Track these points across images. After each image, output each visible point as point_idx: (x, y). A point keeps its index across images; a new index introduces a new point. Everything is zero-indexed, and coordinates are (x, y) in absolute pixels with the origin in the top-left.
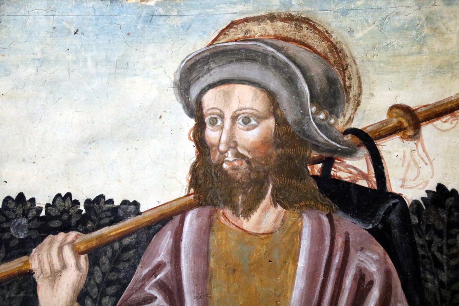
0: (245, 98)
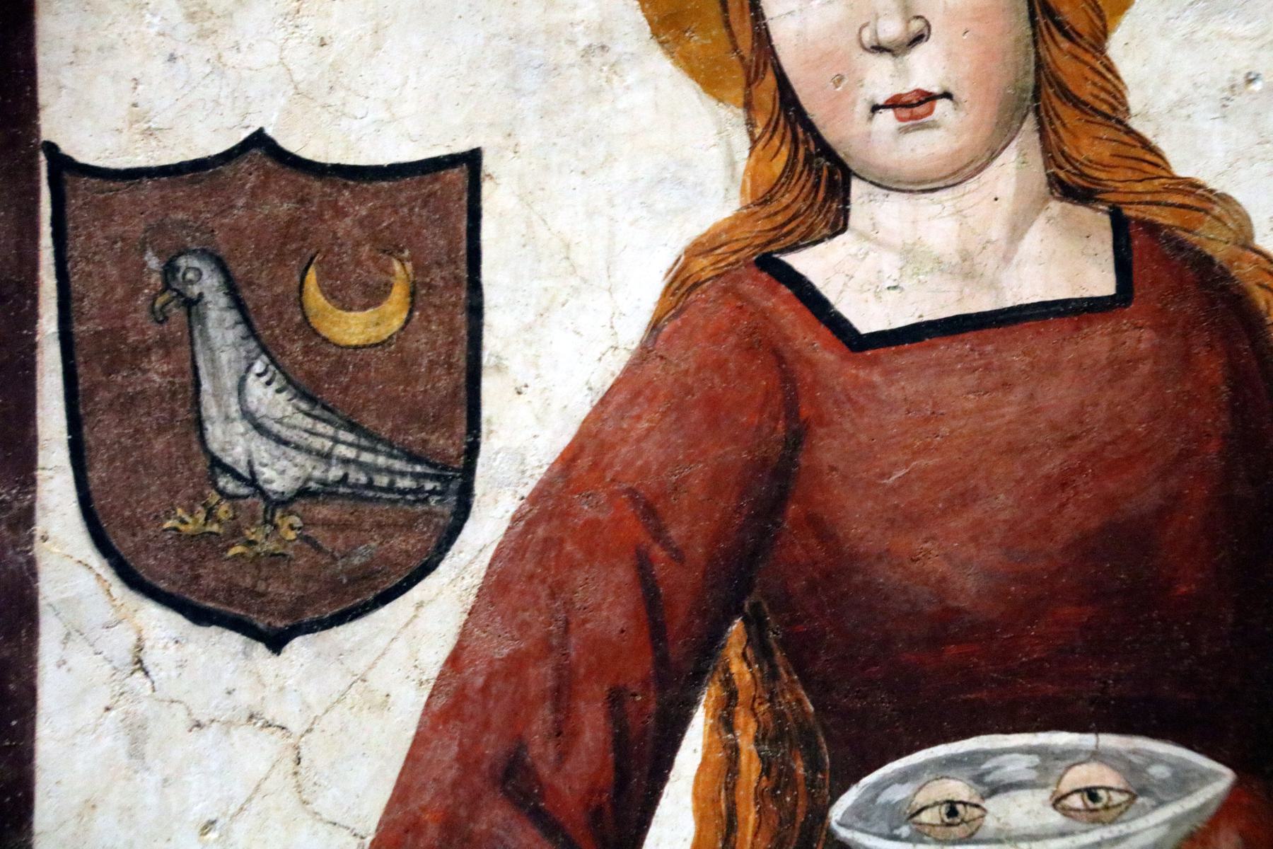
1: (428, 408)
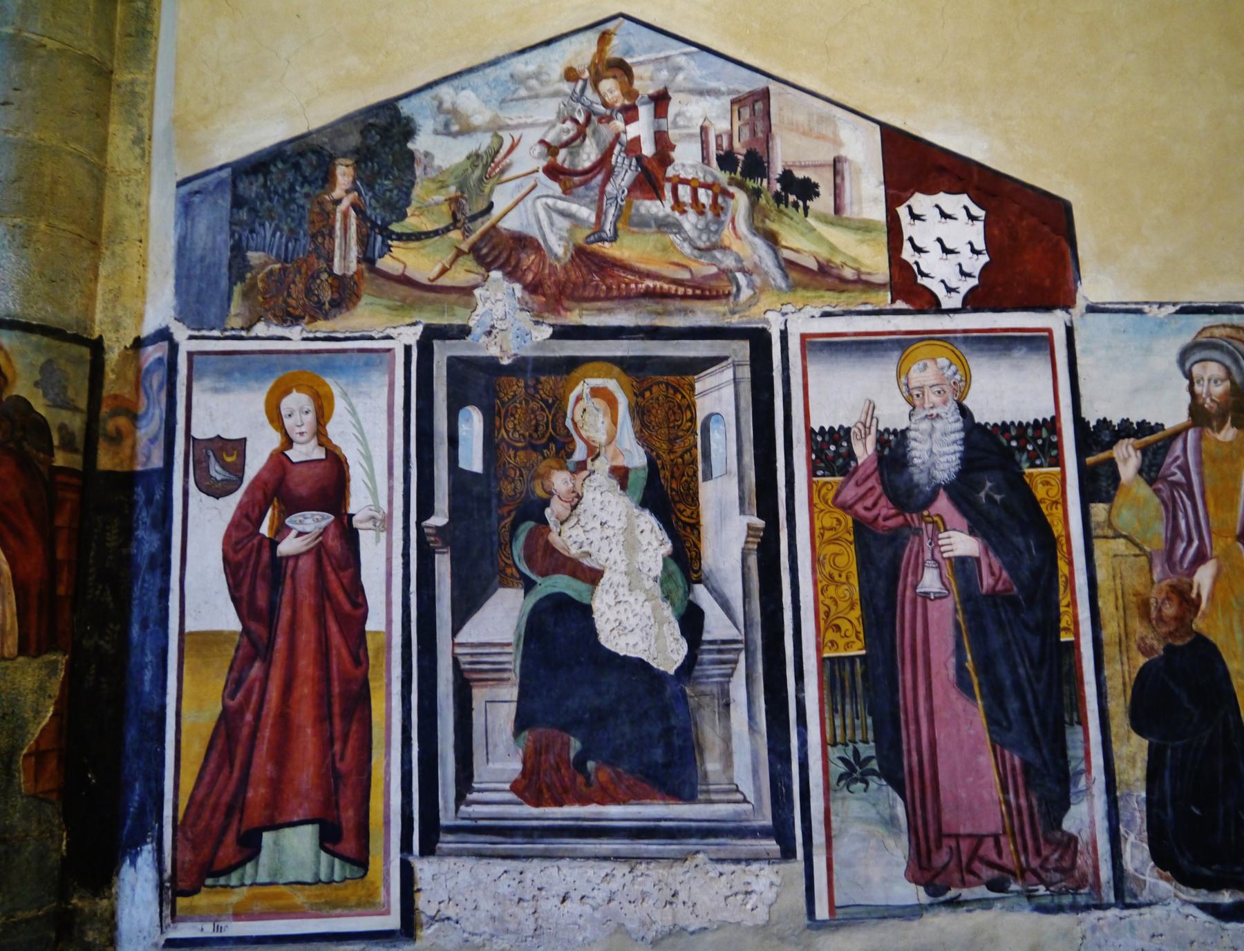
0: (1214, 370)
1: (238, 470)
